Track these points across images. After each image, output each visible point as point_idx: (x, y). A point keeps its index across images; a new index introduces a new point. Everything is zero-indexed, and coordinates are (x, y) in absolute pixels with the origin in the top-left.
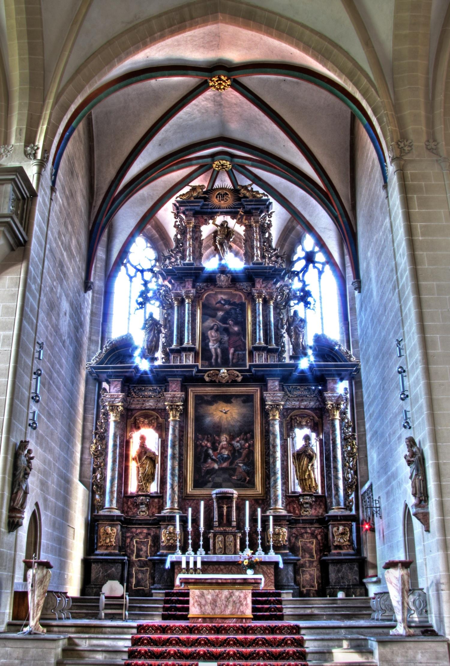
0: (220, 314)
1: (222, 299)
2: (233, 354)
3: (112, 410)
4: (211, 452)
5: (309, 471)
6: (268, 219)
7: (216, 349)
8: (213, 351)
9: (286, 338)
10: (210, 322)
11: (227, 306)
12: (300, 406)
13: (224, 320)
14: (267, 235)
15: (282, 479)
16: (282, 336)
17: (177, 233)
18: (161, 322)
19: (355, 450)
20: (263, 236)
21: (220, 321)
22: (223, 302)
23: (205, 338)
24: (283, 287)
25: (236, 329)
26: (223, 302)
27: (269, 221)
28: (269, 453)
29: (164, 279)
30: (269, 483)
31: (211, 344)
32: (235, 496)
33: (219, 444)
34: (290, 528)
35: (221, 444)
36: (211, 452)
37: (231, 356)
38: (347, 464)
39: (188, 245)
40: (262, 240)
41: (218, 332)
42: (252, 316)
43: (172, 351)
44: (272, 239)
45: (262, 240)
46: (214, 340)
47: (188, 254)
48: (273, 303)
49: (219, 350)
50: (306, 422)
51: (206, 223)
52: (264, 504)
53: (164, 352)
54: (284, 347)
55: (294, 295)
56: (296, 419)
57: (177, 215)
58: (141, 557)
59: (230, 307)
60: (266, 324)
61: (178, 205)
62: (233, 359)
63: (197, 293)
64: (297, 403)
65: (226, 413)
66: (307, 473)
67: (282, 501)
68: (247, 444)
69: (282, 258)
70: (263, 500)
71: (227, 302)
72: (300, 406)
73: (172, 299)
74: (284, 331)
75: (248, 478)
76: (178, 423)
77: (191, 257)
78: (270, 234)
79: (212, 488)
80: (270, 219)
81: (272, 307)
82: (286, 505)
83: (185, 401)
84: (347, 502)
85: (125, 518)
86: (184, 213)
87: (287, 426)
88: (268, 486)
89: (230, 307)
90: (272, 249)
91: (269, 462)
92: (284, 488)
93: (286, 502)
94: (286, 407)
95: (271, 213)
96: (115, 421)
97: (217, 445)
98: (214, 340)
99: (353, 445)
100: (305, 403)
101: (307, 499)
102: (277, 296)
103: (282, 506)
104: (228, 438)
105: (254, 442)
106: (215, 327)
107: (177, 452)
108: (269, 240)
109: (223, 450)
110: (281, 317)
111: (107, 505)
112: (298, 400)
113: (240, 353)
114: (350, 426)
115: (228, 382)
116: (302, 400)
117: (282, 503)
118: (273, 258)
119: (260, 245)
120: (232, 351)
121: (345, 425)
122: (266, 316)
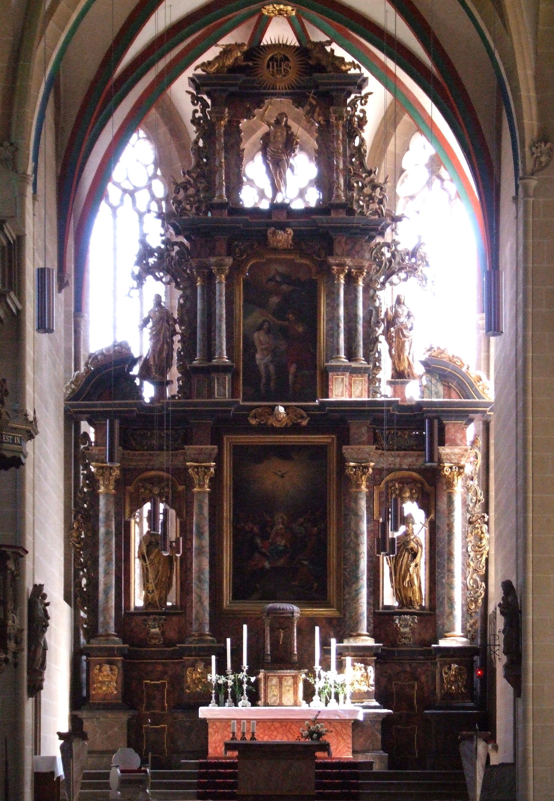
0: (275, 300)
1: (278, 273)
2: (296, 376)
3: (102, 475)
4: (258, 541)
5: (410, 575)
6: (360, 107)
7: (267, 367)
8: (262, 368)
9: (383, 346)
10: (257, 316)
11: (285, 287)
12: (400, 465)
13: (280, 313)
14: (357, 142)
15: (369, 586)
16: (376, 340)
17: (198, 138)
18: (176, 316)
19: (484, 542)
20: (350, 142)
21: (274, 315)
22: (278, 279)
23: (249, 347)
24: (381, 247)
25: (300, 329)
26: (278, 279)
27: (363, 111)
28: (350, 542)
29: (178, 233)
30: (349, 593)
31: (258, 356)
32: (297, 615)
33: (272, 528)
34: (381, 664)
35: (275, 528)
36: (258, 541)
37: (291, 377)
38: (471, 563)
39: (217, 163)
40: (348, 154)
41: (271, 335)
42: (328, 305)
43: (196, 370)
44: (365, 152)
45: (348, 154)
46: (262, 350)
47: (217, 183)
48: (364, 280)
49: (271, 368)
50: (411, 491)
51: (249, 115)
52: (340, 626)
53: (182, 369)
54: (379, 360)
55: (399, 263)
56: (394, 485)
57: (195, 99)
58: (154, 708)
59: (291, 288)
60: (351, 318)
61: (197, 81)
62: (294, 383)
63: (234, 259)
64: (398, 460)
65: (282, 476)
66: (408, 579)
67: (368, 620)
68: (316, 529)
69: (381, 189)
70: (338, 619)
71: (287, 279)
72: (400, 465)
73: (192, 272)
74: (380, 331)
75: (316, 585)
76: (207, 495)
77: (224, 189)
78: (362, 140)
79: (261, 599)
80: (364, 107)
81: (360, 289)
82: (375, 627)
83: (219, 460)
84: (468, 625)
85: (129, 650)
86: (209, 96)
87: (380, 497)
88: (347, 597)
89: (291, 288)
90: (365, 171)
91: (350, 559)
92: (371, 601)
93: (374, 622)
94: (379, 467)
95: (366, 96)
96: (107, 494)
97: (269, 529)
98: (262, 350)
99: (482, 533)
100: (410, 460)
101: (406, 620)
102: (370, 266)
103: (368, 631)
104: (285, 518)
105: (326, 525)
106: (266, 326)
107: (206, 542)
108: (359, 152)
109: (278, 539)
110: (377, 304)
111: (101, 630)
112: (398, 456)
113: (306, 372)
114: (479, 501)
115: (286, 425)
116: (405, 456)
117: (368, 625)
118: (367, 190)
119: (344, 163)
120: (293, 369)
121: (472, 499)
122: (351, 304)
